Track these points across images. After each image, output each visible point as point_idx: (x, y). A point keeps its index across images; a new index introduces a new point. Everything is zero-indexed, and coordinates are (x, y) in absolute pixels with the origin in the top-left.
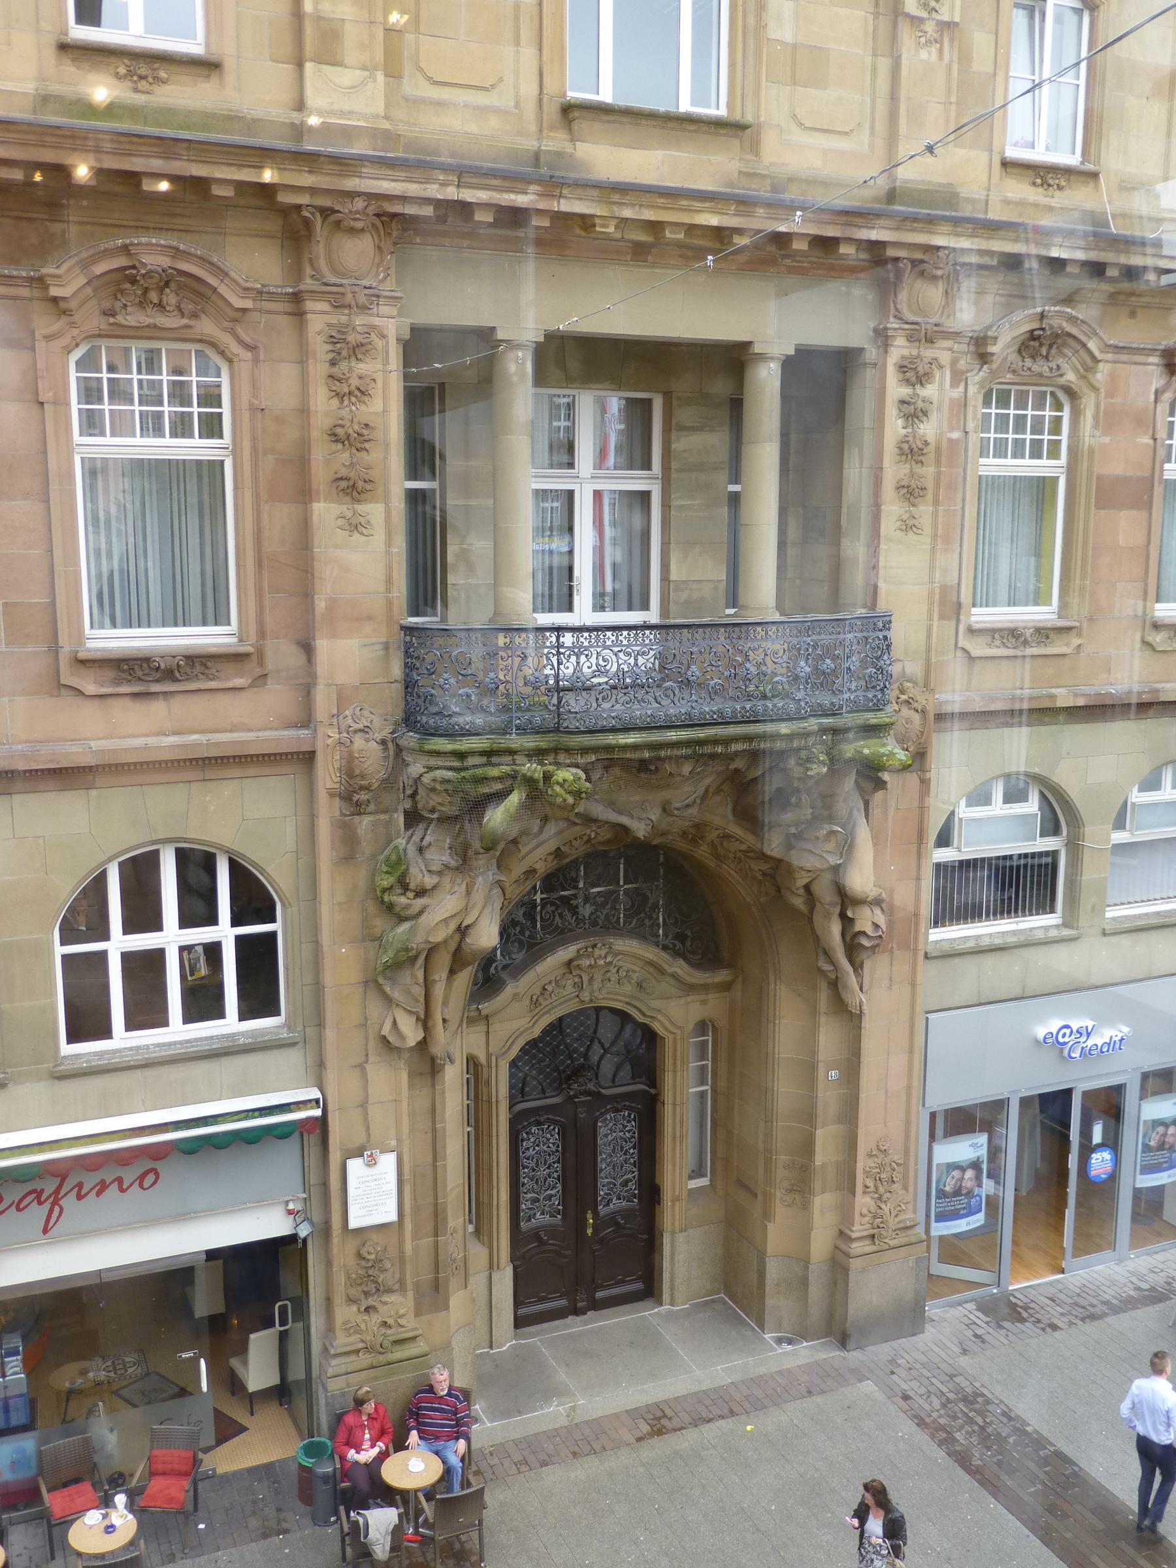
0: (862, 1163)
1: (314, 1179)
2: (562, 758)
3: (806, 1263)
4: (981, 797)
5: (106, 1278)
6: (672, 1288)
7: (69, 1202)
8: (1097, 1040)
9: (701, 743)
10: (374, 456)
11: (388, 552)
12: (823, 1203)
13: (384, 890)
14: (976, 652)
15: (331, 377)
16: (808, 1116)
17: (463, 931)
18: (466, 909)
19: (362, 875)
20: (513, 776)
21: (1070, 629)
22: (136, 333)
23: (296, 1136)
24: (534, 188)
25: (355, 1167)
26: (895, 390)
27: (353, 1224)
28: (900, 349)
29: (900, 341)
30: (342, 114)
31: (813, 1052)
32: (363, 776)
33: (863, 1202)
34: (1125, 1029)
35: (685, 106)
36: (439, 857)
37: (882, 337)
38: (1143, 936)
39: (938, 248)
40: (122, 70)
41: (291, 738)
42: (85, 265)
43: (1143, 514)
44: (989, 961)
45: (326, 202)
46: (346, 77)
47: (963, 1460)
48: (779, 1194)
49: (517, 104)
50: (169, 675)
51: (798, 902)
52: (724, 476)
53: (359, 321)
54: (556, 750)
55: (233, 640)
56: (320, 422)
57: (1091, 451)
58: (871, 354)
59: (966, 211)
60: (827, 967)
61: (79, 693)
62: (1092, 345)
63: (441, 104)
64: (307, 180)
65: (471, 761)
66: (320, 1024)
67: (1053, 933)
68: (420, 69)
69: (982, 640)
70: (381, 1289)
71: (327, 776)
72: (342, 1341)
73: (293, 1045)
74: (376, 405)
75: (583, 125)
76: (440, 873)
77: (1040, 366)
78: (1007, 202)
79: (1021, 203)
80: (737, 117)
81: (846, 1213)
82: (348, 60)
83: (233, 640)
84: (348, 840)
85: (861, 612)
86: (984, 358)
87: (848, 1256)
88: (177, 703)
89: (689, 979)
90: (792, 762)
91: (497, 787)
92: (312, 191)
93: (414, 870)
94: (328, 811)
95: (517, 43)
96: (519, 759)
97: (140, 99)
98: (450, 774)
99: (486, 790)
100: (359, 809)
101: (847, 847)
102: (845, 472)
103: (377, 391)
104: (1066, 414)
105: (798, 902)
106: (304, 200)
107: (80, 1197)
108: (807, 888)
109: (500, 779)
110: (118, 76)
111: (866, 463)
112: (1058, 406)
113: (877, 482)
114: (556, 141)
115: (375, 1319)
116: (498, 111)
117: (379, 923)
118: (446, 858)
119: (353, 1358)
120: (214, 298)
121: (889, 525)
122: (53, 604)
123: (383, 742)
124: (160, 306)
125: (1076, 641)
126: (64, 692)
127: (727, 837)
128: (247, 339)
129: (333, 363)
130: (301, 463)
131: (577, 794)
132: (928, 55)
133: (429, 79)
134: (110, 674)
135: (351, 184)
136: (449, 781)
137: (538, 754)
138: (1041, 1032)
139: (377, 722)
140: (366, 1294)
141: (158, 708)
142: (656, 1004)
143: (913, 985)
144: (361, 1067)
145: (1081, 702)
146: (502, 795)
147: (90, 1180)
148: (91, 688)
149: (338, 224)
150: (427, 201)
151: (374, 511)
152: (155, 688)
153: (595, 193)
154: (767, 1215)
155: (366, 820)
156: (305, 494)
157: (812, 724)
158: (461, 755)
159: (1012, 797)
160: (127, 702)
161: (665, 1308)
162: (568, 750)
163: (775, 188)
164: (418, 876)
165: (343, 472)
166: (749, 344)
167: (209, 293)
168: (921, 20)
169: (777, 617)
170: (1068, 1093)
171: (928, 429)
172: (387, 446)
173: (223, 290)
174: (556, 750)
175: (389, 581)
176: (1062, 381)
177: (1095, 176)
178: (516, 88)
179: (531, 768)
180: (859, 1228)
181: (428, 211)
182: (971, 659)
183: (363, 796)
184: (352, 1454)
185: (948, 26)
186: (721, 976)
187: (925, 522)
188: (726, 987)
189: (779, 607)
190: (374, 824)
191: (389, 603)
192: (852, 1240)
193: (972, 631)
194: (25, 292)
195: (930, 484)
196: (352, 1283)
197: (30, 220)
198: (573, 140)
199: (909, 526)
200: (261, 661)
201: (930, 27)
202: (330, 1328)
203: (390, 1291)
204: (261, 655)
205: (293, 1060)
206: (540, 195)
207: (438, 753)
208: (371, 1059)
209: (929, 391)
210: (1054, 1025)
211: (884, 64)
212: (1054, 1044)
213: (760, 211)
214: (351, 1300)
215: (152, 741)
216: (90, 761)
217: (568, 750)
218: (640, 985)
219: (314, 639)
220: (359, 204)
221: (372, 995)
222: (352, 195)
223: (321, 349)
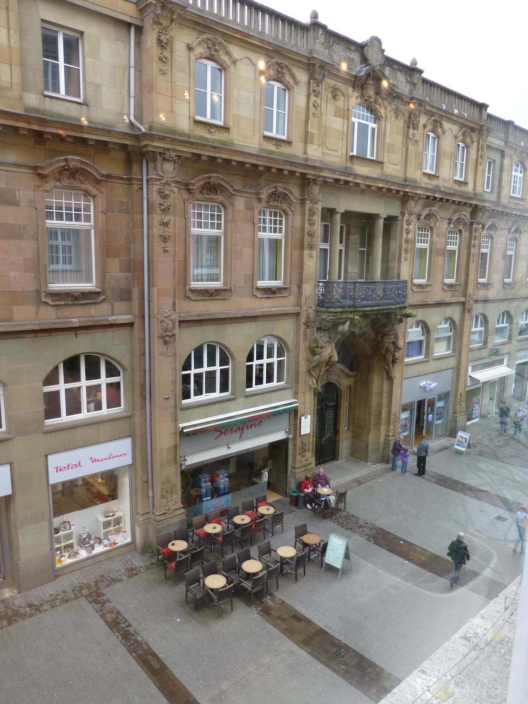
0: (392, 417)
1: (292, 423)
2: (356, 313)
3: (379, 444)
4: (411, 327)
5: (250, 451)
6: (341, 456)
7: (245, 430)
8: (432, 386)
9: (380, 310)
10: (315, 239)
11: (316, 263)
12: (383, 428)
13: (314, 347)
14: (415, 290)
15: (309, 220)
16: (380, 406)
17: (330, 357)
18: (332, 352)
19: (307, 344)
20: (347, 318)
21: (430, 285)
22: (272, 207)
23: (288, 413)
24: (353, 176)
25: (303, 418)
26: (405, 227)
27: (302, 434)
28: (406, 217)
29: (407, 215)
30: (314, 156)
31: (382, 389)
32: (310, 319)
33: (392, 427)
34: (436, 384)
35: (368, 157)
36: (326, 339)
37: (403, 214)
38: (440, 360)
39: (417, 194)
40: (274, 143)
41: (296, 309)
42: (268, 190)
43: (443, 258)
44: (414, 366)
45: (315, 178)
46: (314, 147)
47: (430, 481)
48: (372, 427)
49: (342, 155)
50: (274, 293)
51: (383, 351)
52: (358, 246)
53: (315, 206)
54: (354, 312)
55: (282, 284)
56: (306, 231)
57: (435, 242)
58: (400, 218)
59: (418, 185)
60: (387, 368)
61: (257, 297)
62: (438, 217)
63: (329, 154)
64: (313, 172)
65: (338, 314)
66: (298, 383)
67: (422, 360)
68: (325, 146)
69: (416, 287)
70: (305, 451)
71: (303, 319)
72: (298, 465)
73: (289, 388)
74: (316, 227)
75: (355, 161)
76: (325, 343)
77: (427, 222)
78: (424, 182)
79: (426, 183)
80: (379, 160)
81: (388, 430)
82: (315, 143)
83: (282, 284)
84: (305, 335)
85: (396, 280)
86: (419, 219)
87: (390, 440)
88: (274, 300)
89: (349, 374)
90: (393, 315)
91: (344, 320)
92: (313, 175)
93: (320, 342)
94: (303, 327)
95: (343, 140)
96: (348, 314)
97: (277, 150)
98: (333, 318)
99: (341, 321)
100: (308, 327)
101: (396, 336)
102: (391, 246)
103: (316, 223)
104: (429, 233)
105: (383, 351)
106: (311, 177)
107: (247, 429)
108: (387, 348)
109: (344, 318)
110: (273, 144)
111: (398, 244)
112: (428, 231)
113: (400, 248)
114: (349, 164)
115: (304, 458)
116: (339, 157)
117: (310, 356)
118: (327, 339)
119: (300, 469)
120: (288, 199)
121: (403, 259)
122: (253, 274)
123: (314, 310)
124: (278, 201)
125: (432, 288)
126: (254, 297)
127: (369, 335)
128: (292, 209)
129: (309, 216)
130: (302, 241)
131: (359, 322)
132: (412, 147)
133: (327, 148)
134: (262, 292)
135: (322, 174)
136: (333, 319)
137: (351, 312)
138: (422, 384)
139: (312, 305)
140: (302, 452)
141: (270, 300)
142: (342, 381)
143: (402, 372)
144: (304, 393)
145: (433, 303)
146: (345, 322)
147: (249, 424)
148: (259, 296)
149: (315, 183)
150: (332, 178)
151: (314, 253)
152: (271, 296)
153: (362, 178)
154: (369, 432)
155: (309, 330)
156: (302, 248)
157: (398, 306)
158: (336, 313)
159: (417, 326)
160: (264, 299)
161: (340, 461)
162: (357, 311)
163: (386, 177)
164: (321, 343)
165: (310, 243)
166: (379, 214)
167: (287, 197)
168: (411, 139)
169: (381, 280)
170: (425, 400)
171: (410, 236)
172: (318, 237)
173: (291, 198)
174: (354, 312)
175: (316, 270)
176: (431, 225)
177: (438, 177)
178: (342, 152)
179: (350, 316)
180: (391, 434)
181: (332, 181)
182: (414, 292)
183: (310, 324)
184: (306, 490)
185: (416, 141)
186: (354, 373)
187: (409, 258)
188: (355, 376)
189: (381, 278)
190: (310, 331)
191: (316, 276)
192: (390, 436)
193: (414, 285)
194: (253, 196)
195: (409, 249)
196: (300, 450)
197: (255, 178)
198: (353, 164)
199: (406, 259)
200: (290, 290)
201: (413, 141)
202: (294, 461)
203: (307, 451)
204: (290, 288)
205: (289, 392)
206: (353, 178)
207: (331, 312)
208: (307, 391)
209: (410, 227)
210: (424, 383)
211: (404, 149)
212: (424, 388)
213: (390, 184)
214: (300, 454)
215: (273, 309)
216: (259, 314)
217: (357, 311)
218: (339, 376)
219: (302, 284)
220: (321, 178)
221: (307, 374)
222: (320, 176)
223: (307, 212)
